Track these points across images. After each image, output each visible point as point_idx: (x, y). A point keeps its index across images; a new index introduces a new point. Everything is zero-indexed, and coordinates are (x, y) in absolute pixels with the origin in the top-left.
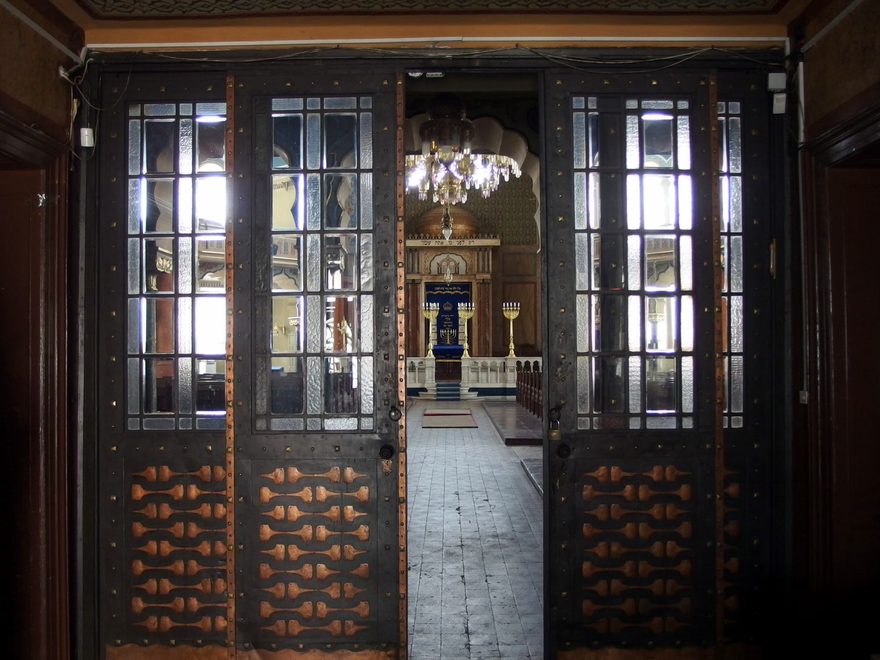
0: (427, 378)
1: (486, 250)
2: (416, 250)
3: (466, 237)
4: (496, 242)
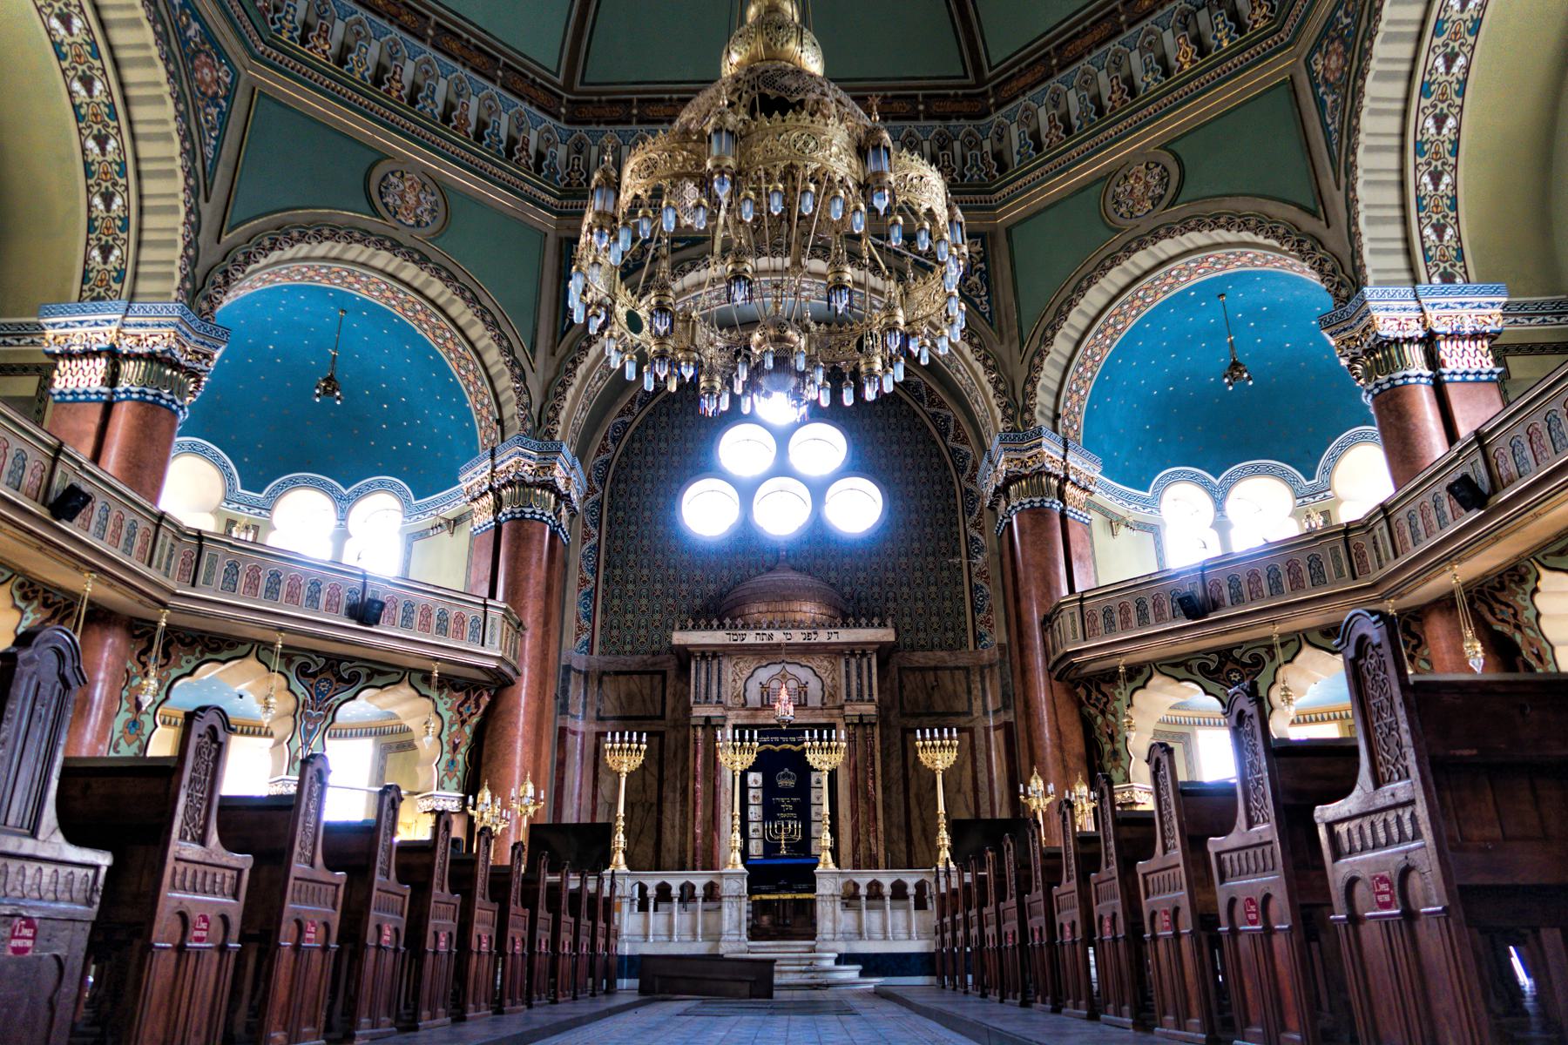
0: (726, 925)
1: (864, 654)
2: (715, 656)
4: (886, 635)
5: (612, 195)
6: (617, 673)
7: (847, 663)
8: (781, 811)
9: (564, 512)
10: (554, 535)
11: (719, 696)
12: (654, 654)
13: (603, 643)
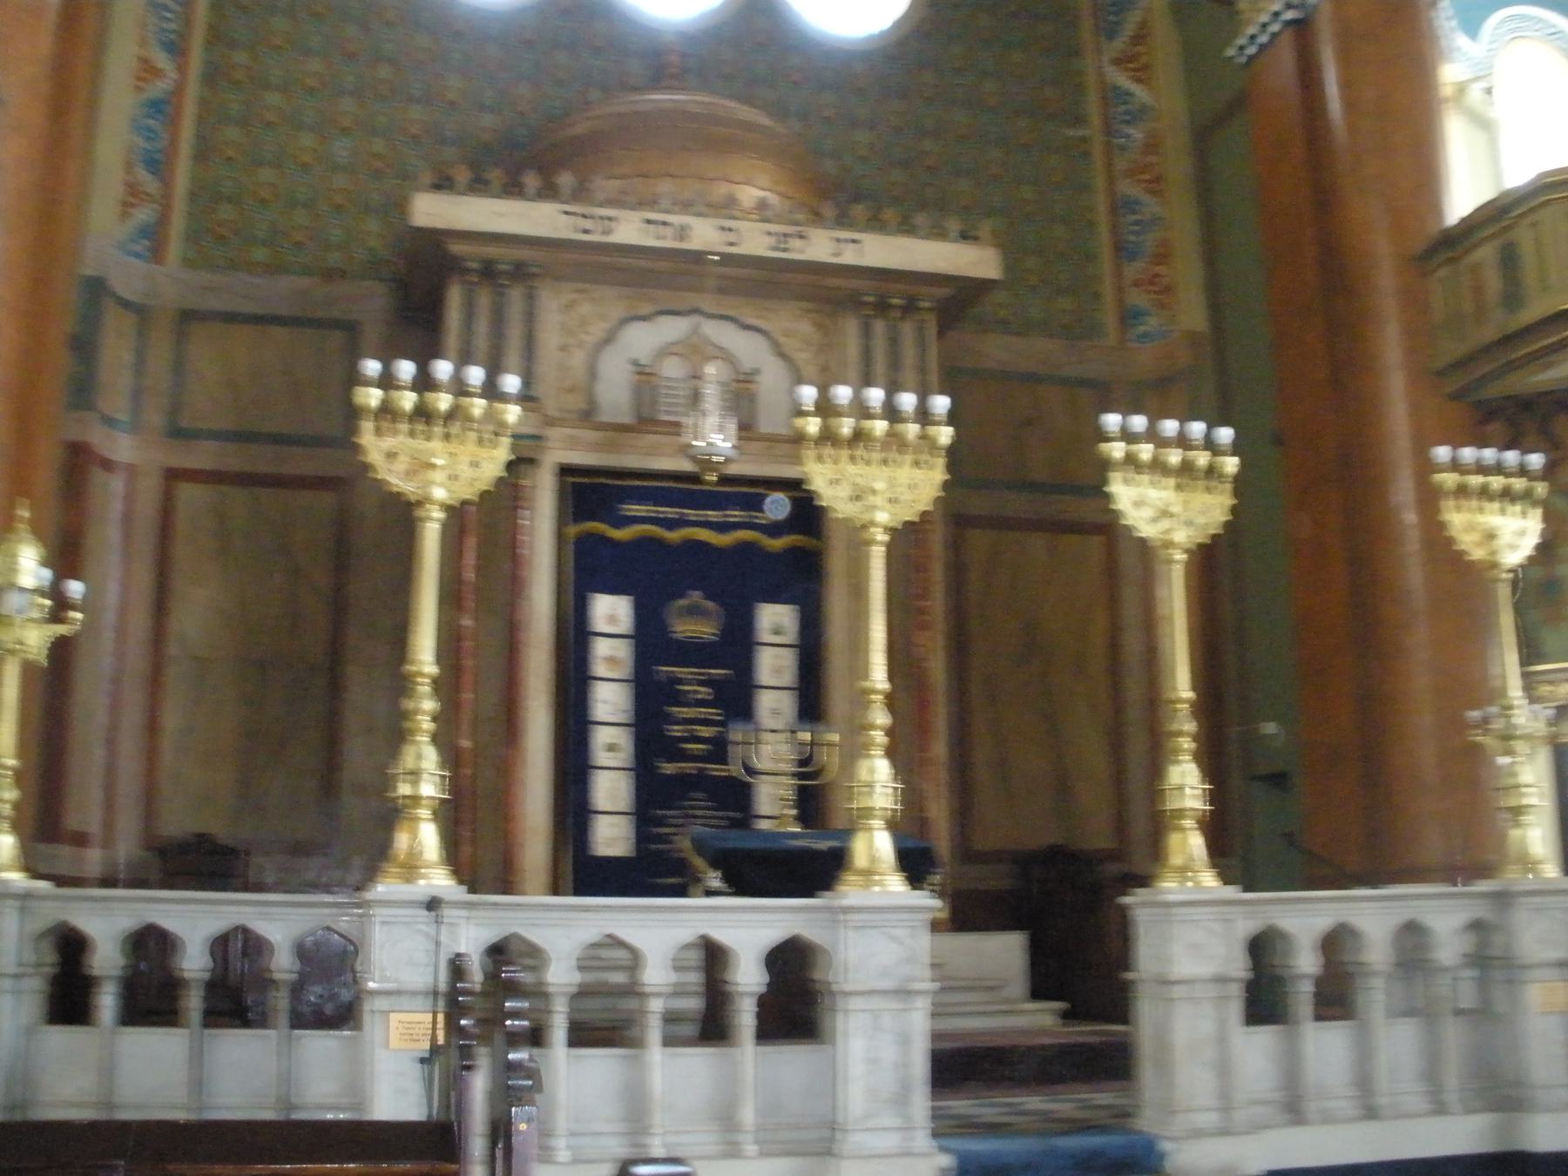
6: (230, 318)
7: (866, 332)
8: (679, 700)
12: (330, 275)
13: (192, 237)
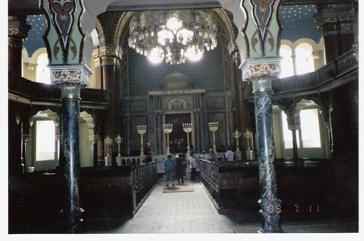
3: (186, 88)
4: (203, 91)
5: (137, 23)
9: (118, 62)
10: (116, 68)
11: (161, 107)
